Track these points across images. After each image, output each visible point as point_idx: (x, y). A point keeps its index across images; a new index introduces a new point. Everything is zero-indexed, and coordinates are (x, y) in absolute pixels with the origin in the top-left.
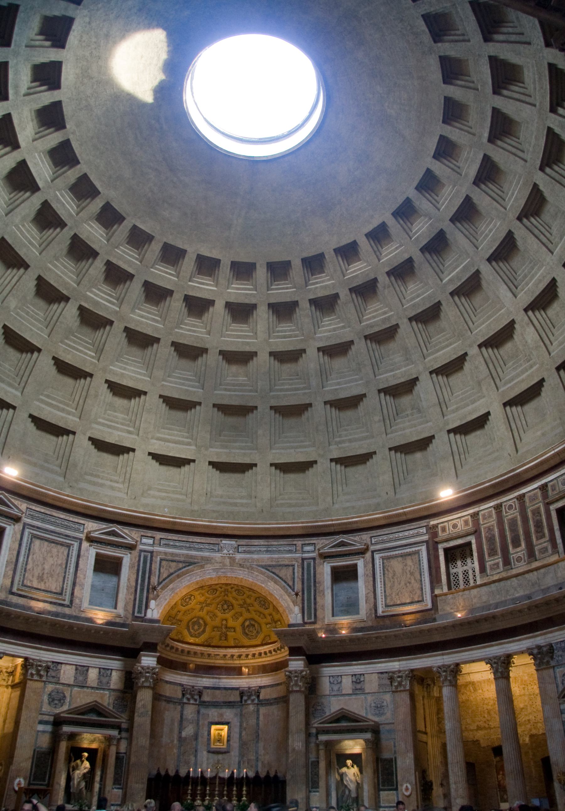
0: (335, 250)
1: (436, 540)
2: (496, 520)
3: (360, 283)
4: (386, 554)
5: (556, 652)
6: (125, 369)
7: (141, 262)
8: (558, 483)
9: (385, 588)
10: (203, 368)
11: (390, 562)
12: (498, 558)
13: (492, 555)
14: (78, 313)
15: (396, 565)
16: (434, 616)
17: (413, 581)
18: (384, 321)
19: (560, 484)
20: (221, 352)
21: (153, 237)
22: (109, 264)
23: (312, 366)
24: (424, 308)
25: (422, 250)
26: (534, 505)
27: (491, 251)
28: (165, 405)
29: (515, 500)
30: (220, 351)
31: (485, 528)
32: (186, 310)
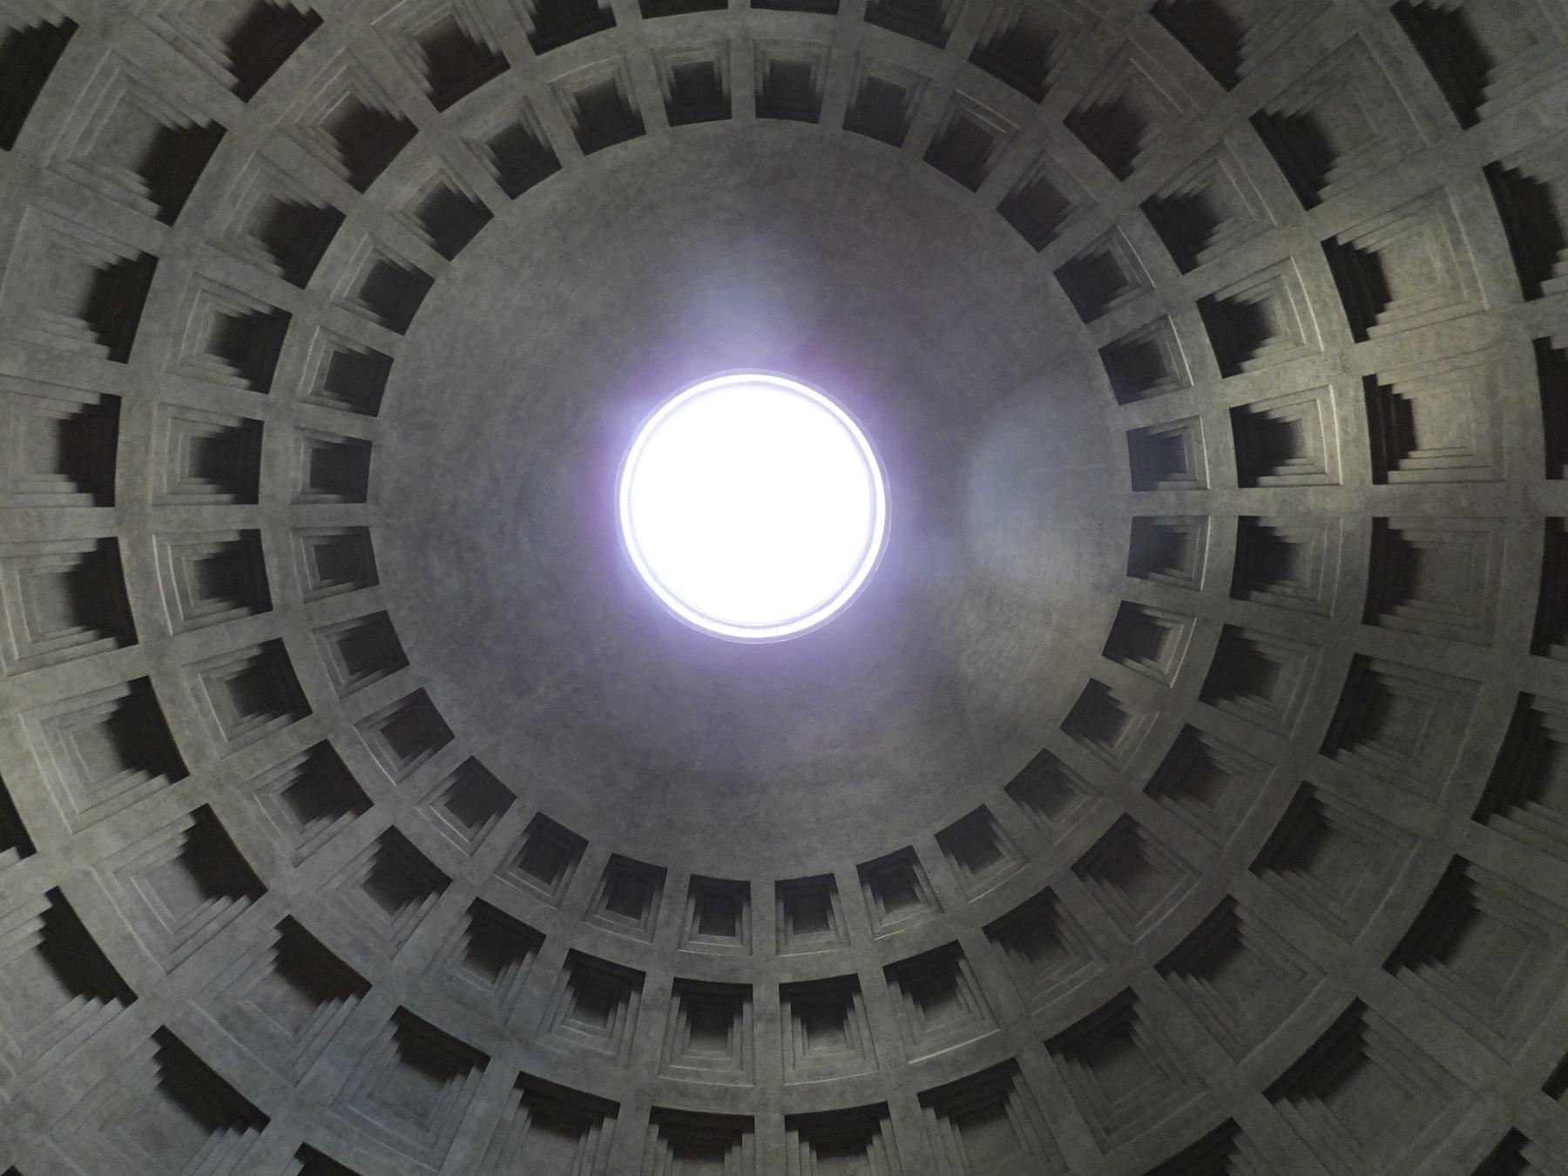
0: (695, 879)
3: (709, 980)
6: (43, 756)
7: (305, 602)
10: (214, 926)
14: (90, 547)
18: (721, 1095)
20: (290, 927)
21: (376, 582)
22: (251, 538)
23: (480, 1107)
24: (840, 1106)
25: (894, 972)
27: (1064, 1025)
28: (39, 925)
30: (289, 919)
32: (293, 776)
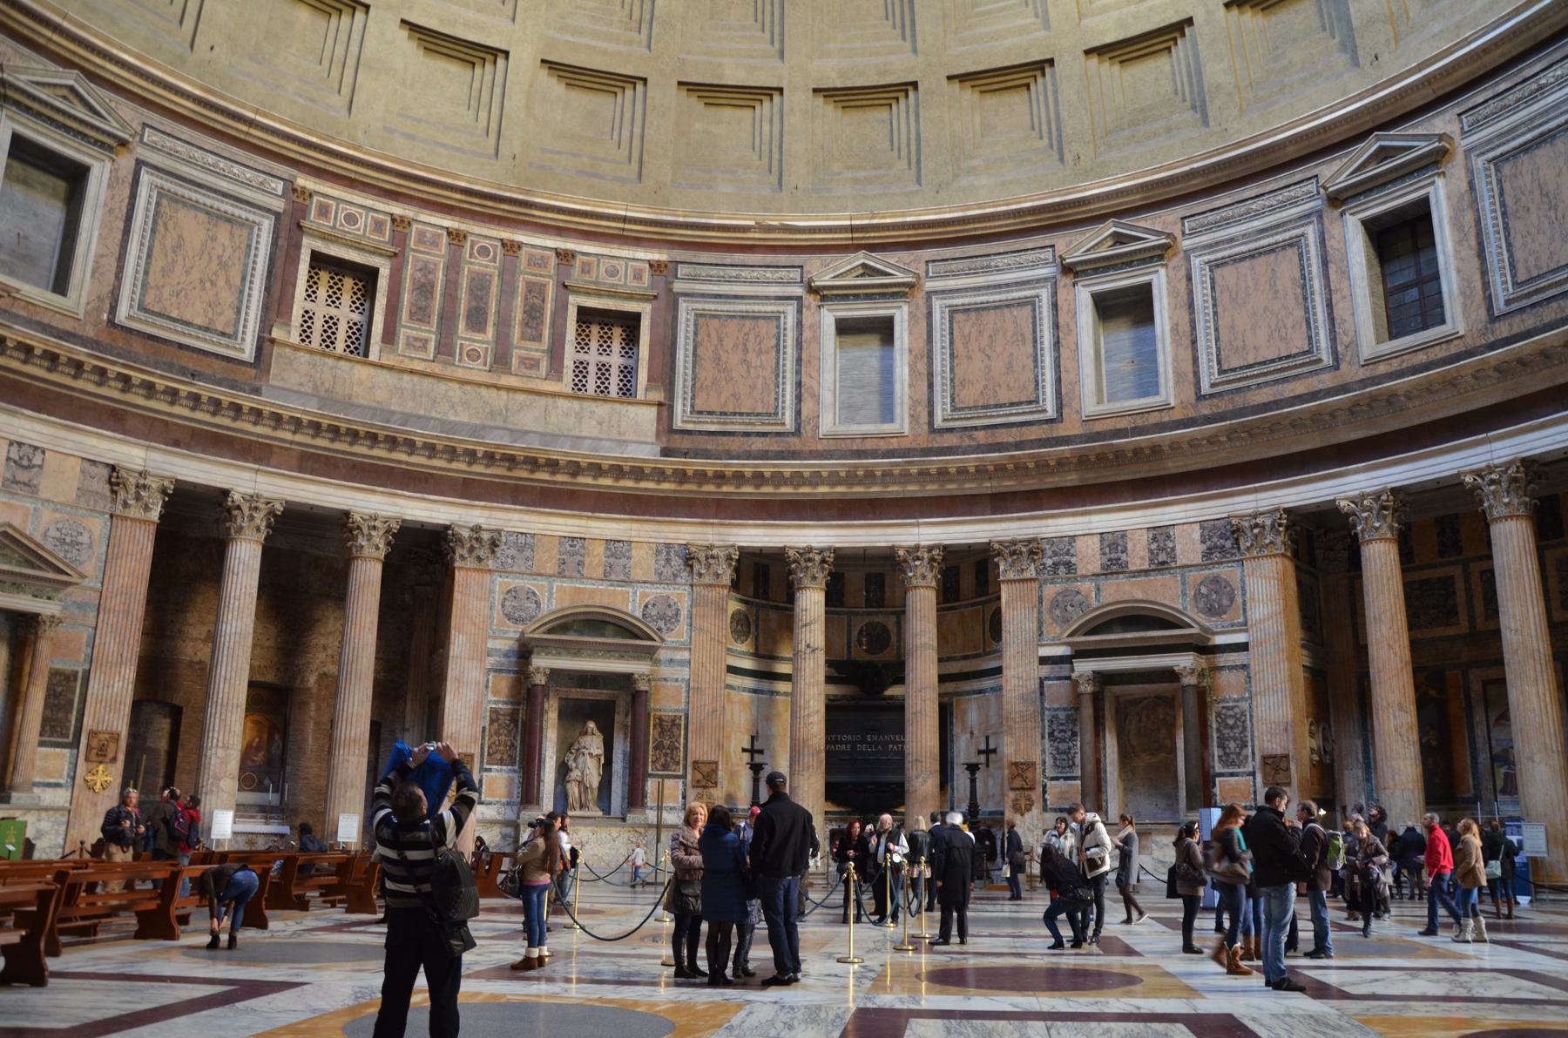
1: (303, 223)
2: (446, 259)
4: (173, 188)
5: (503, 547)
8: (598, 265)
9: (148, 264)
11: (177, 212)
12: (429, 332)
13: (418, 320)
15: (191, 226)
16: (258, 384)
17: (221, 283)
19: (602, 269)
26: (535, 275)
29: (499, 244)
31: (416, 260)
